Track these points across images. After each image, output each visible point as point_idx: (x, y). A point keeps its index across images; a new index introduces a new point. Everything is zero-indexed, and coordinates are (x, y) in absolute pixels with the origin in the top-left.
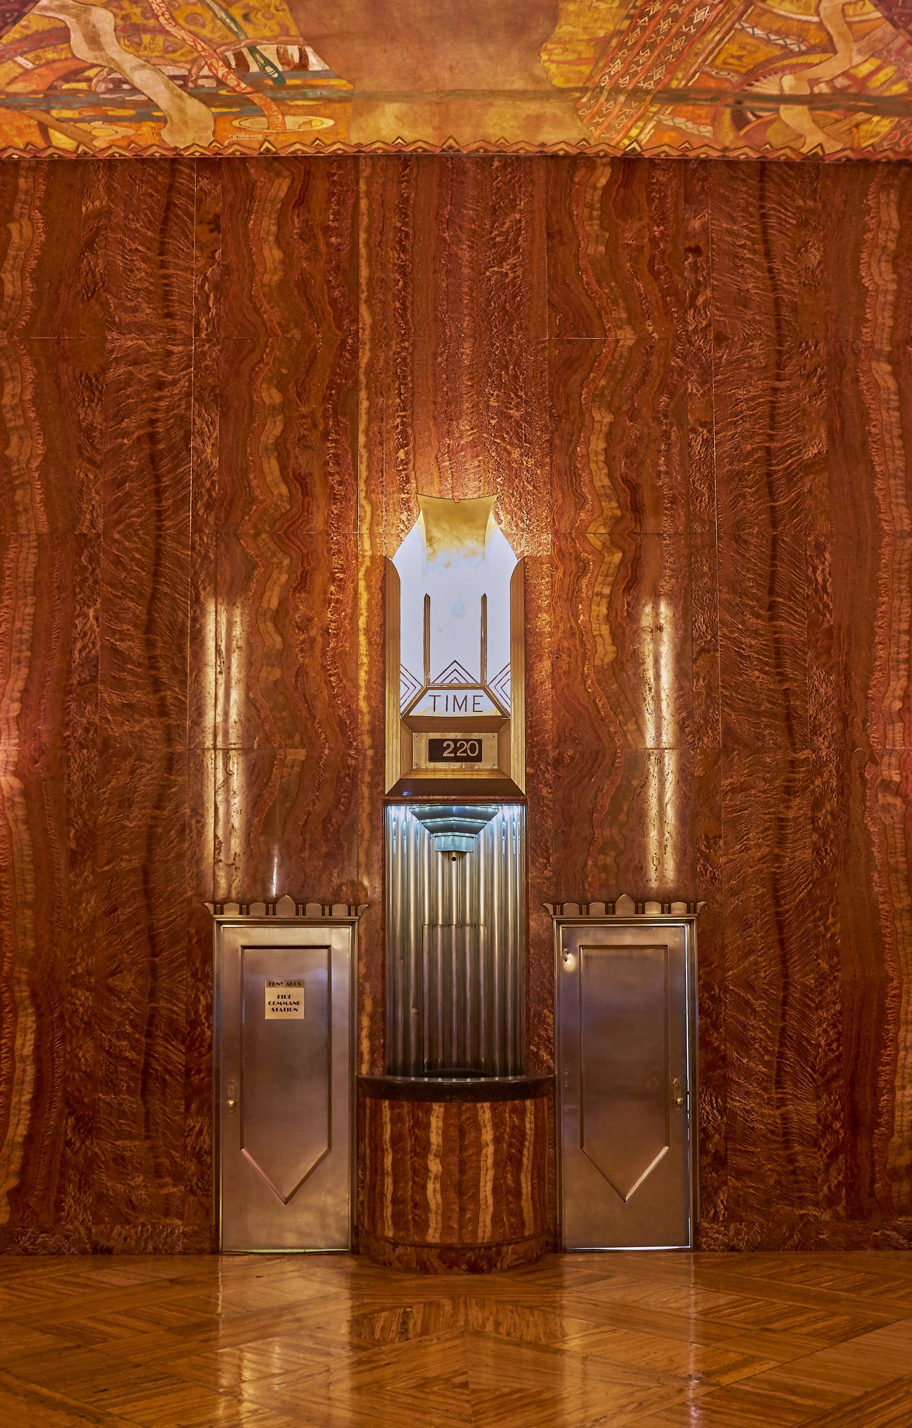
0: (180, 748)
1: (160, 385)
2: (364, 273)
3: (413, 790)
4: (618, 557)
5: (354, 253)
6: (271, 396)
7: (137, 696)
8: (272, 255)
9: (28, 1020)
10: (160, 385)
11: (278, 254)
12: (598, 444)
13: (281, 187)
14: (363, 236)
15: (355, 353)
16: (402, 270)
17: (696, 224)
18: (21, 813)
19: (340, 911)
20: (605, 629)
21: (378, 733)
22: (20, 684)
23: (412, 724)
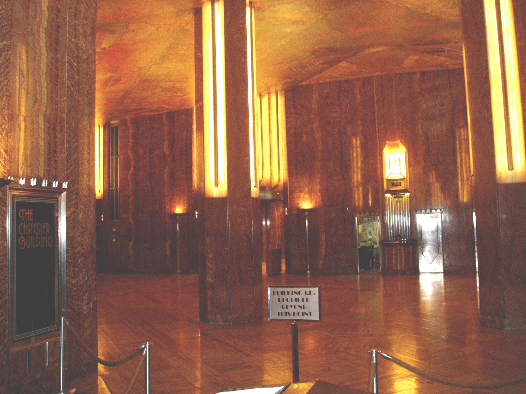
0: (347, 186)
1: (340, 122)
2: (375, 98)
3: (388, 192)
4: (424, 147)
5: (373, 95)
6: (360, 122)
7: (340, 177)
8: (359, 96)
9: (324, 234)
10: (340, 122)
11: (360, 96)
12: (420, 126)
13: (360, 84)
14: (375, 92)
15: (374, 113)
16: (382, 97)
17: (437, 83)
18: (321, 199)
19: (377, 213)
20: (423, 160)
21: (382, 182)
22: (319, 176)
23: (388, 180)
